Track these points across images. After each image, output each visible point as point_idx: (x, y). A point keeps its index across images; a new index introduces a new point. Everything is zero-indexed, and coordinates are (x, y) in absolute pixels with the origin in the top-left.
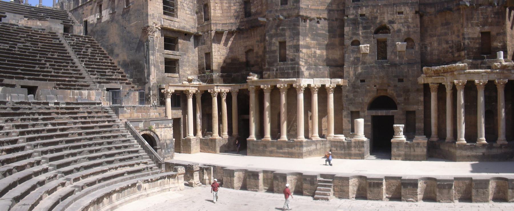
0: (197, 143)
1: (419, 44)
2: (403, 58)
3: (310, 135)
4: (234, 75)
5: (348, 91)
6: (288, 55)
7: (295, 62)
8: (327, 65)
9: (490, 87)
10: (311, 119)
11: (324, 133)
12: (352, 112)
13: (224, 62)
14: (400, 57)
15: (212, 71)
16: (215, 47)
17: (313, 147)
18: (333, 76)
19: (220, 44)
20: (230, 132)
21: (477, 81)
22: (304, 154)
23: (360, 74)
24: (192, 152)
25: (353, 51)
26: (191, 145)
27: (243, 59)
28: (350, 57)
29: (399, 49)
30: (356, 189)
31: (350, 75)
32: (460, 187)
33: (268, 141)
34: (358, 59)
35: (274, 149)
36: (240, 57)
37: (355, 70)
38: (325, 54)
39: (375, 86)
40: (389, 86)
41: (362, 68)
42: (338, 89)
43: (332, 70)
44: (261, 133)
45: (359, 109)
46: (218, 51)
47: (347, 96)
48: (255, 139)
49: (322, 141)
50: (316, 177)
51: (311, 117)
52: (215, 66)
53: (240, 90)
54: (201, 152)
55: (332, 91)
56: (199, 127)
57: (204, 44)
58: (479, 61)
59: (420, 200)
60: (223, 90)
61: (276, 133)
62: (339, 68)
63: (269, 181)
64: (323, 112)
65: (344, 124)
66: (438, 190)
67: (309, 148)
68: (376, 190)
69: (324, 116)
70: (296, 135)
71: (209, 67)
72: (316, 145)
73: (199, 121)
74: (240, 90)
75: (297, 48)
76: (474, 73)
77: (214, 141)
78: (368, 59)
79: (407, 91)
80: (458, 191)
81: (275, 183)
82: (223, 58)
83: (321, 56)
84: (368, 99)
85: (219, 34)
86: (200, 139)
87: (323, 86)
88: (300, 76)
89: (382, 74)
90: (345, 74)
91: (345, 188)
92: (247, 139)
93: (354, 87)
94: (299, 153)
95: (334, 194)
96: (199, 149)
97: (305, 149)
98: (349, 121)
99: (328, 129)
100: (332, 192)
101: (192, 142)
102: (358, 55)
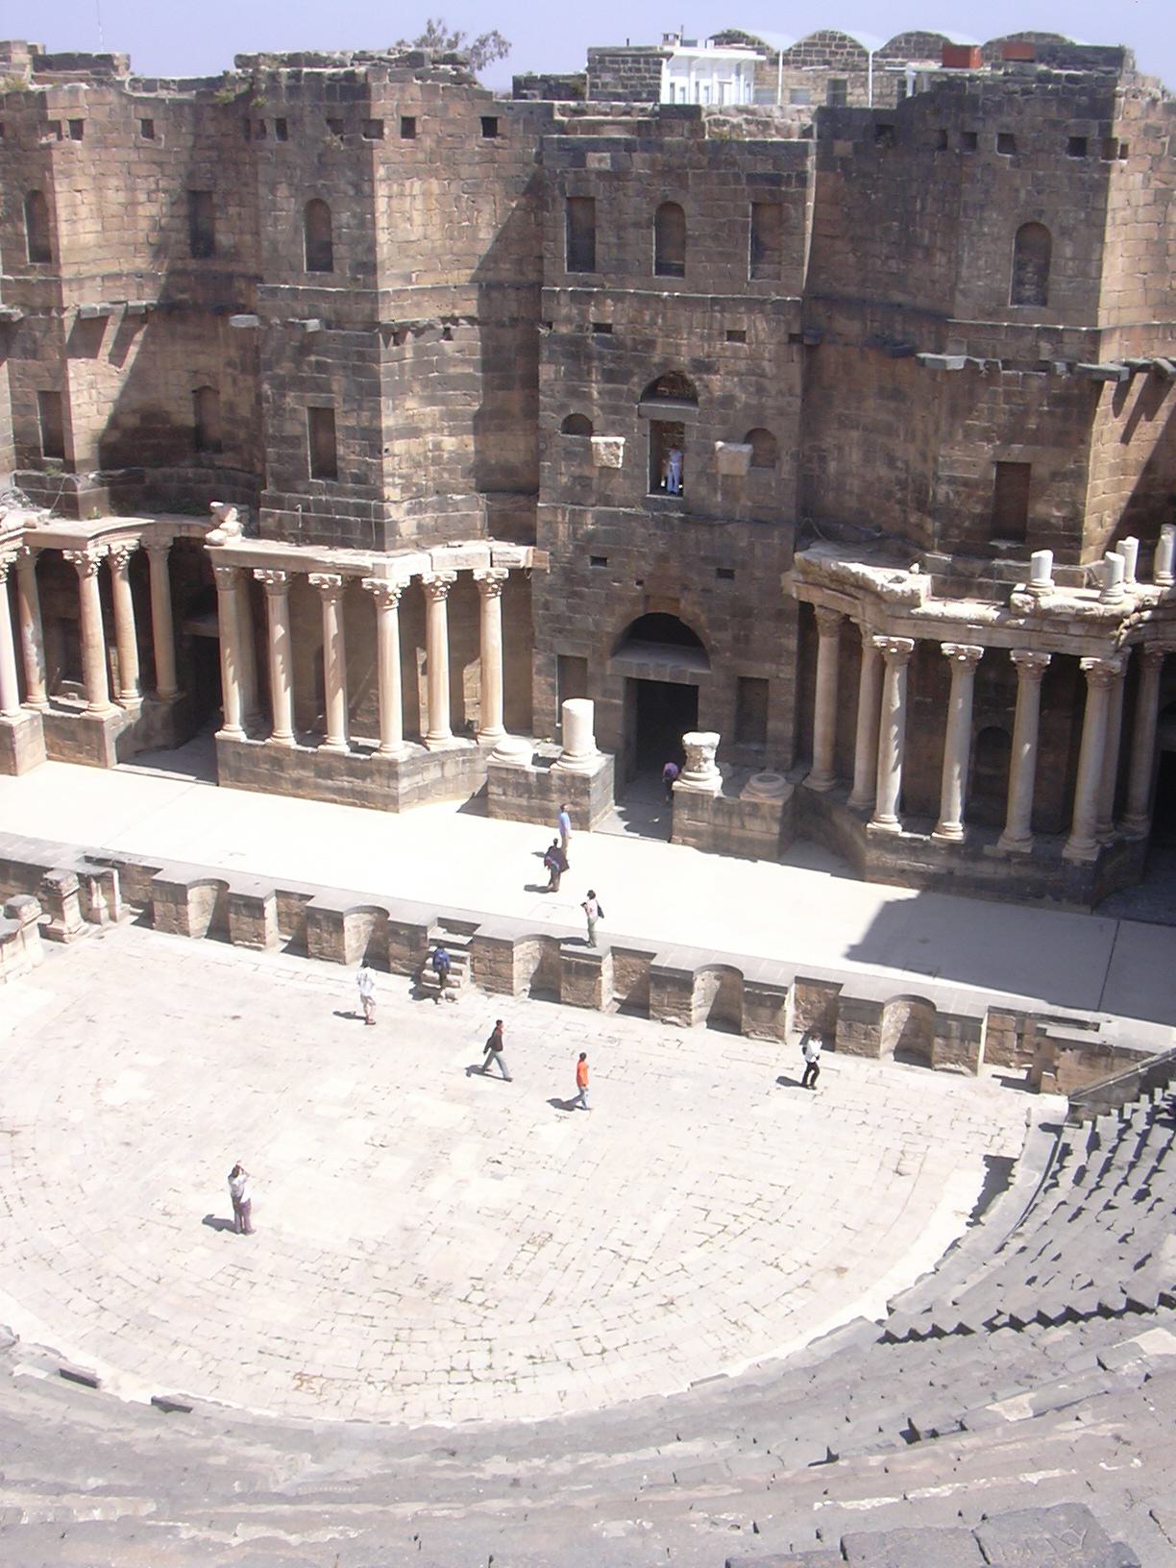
0: (34, 732)
1: (795, 457)
2: (737, 499)
3: (424, 725)
4: (153, 474)
5: (551, 589)
6: (343, 459)
7: (369, 485)
8: (482, 489)
9: (995, 671)
10: (424, 673)
11: (470, 715)
12: (562, 658)
13: (114, 422)
14: (725, 494)
15: (70, 466)
16: (79, 371)
17: (433, 773)
18: (503, 528)
19: (94, 356)
20: (148, 681)
21: (947, 648)
22: (401, 800)
23: (591, 537)
24: (20, 770)
25: (569, 455)
26: (18, 747)
27: (185, 416)
28: (558, 474)
29: (724, 467)
30: (532, 968)
31: (556, 536)
32: (811, 1003)
33: (287, 750)
34: (583, 481)
35: (307, 774)
36: (171, 407)
37: (576, 518)
38: (472, 448)
39: (640, 583)
40: (685, 588)
41: (598, 519)
42: (518, 577)
43: (497, 506)
44: (260, 717)
45: (586, 654)
46: (92, 385)
47: (546, 606)
48: (243, 737)
49: (463, 751)
50: (424, 929)
51: (424, 666)
52: (81, 447)
53: (175, 539)
54: (49, 758)
55: (495, 591)
56: (36, 673)
57: (33, 353)
58: (978, 565)
59: (699, 1020)
60: (116, 547)
61: (311, 723)
62: (522, 500)
63: (295, 919)
64: (466, 647)
65: (536, 693)
66: (744, 1005)
67: (418, 778)
68: (583, 983)
69: (471, 661)
70: (375, 729)
71: (57, 443)
72: (443, 765)
73: (33, 653)
74: (175, 539)
75: (373, 441)
76: (943, 620)
77: (95, 726)
78: (620, 487)
79: (743, 613)
80: (804, 1012)
81: (312, 932)
82: (108, 409)
83: (457, 457)
84: (613, 624)
85: (90, 328)
86: (46, 717)
87: (465, 575)
88: (387, 540)
89: (661, 546)
90: (541, 533)
91: (502, 968)
92: (218, 734)
93: (570, 577)
94: (387, 796)
95: (474, 980)
96: (43, 751)
97: (404, 785)
98: (552, 686)
99: (482, 703)
100: (467, 972)
101: (18, 736)
102: (586, 472)
